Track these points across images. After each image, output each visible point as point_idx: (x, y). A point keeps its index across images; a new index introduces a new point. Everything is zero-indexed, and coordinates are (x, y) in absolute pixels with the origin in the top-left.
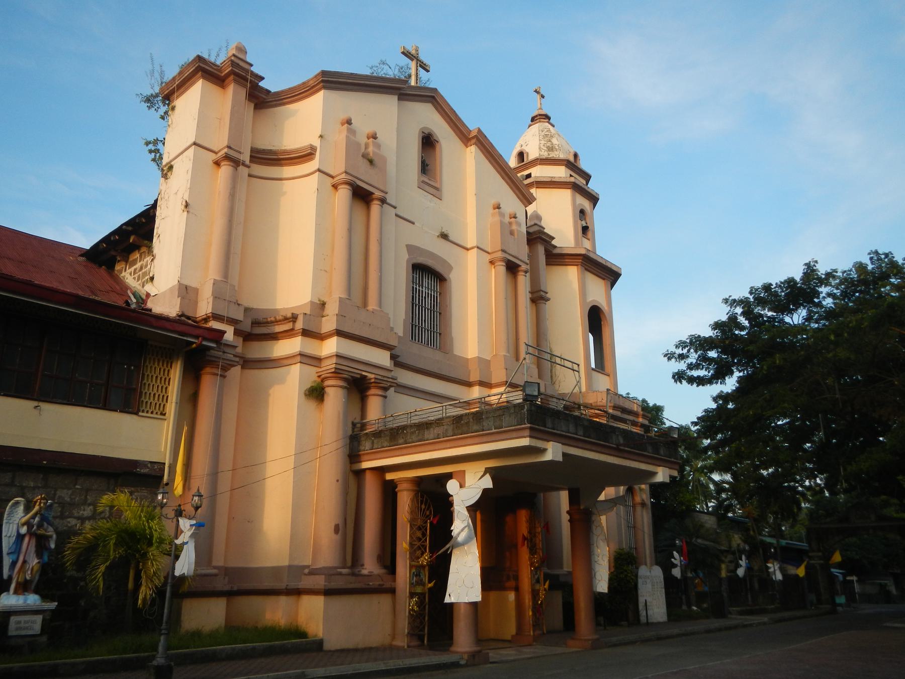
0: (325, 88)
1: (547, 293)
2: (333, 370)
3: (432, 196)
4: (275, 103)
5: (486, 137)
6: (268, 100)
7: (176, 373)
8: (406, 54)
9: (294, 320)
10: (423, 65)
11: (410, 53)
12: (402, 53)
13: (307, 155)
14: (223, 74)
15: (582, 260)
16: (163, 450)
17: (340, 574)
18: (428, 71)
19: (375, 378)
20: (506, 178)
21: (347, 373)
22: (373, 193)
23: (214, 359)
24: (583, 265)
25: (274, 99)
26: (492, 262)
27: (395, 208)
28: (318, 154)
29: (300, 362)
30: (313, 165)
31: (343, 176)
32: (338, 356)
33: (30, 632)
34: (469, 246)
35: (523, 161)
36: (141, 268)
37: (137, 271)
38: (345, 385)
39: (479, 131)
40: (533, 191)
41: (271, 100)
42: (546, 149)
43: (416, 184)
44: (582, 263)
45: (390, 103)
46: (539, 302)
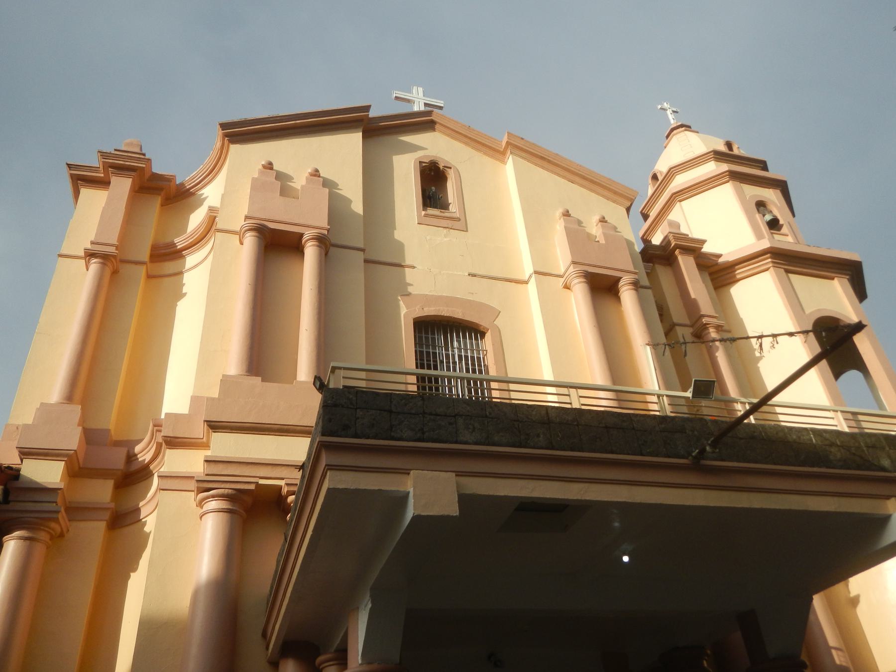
0: (233, 142)
5: (522, 139)
15: (771, 258)
19: (287, 484)
20: (577, 179)
21: (223, 486)
23: (15, 515)
24: (776, 265)
26: (567, 287)
27: (363, 250)
34: (526, 278)
35: (658, 180)
38: (230, 507)
43: (417, 222)
44: (773, 262)
46: (704, 334)
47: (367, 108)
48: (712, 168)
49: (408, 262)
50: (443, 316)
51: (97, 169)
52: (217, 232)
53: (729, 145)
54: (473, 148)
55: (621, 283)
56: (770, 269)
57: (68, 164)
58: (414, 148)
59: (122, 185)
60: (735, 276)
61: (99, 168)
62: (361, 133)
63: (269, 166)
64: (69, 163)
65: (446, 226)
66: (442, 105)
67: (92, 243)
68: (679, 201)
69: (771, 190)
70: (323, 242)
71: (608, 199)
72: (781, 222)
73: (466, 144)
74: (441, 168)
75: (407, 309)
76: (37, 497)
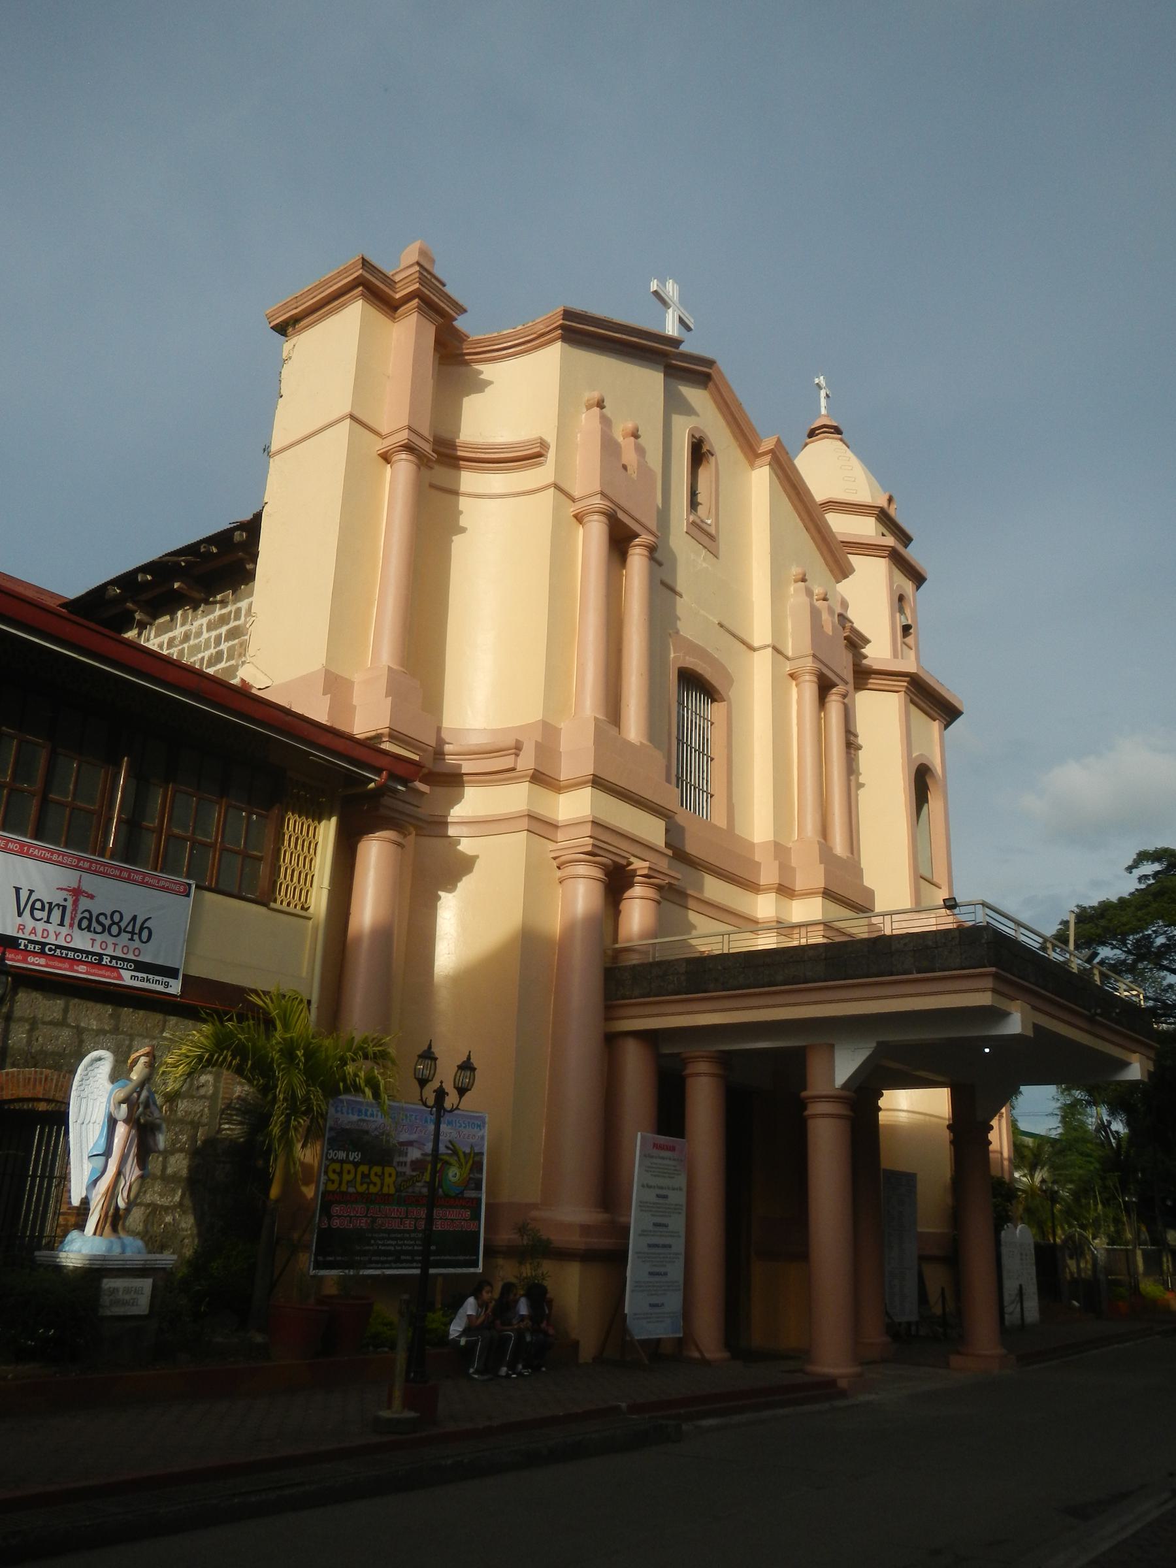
2: (589, 848)
7: (327, 832)
9: (517, 751)
13: (532, 456)
14: (397, 296)
15: (908, 683)
16: (304, 974)
24: (908, 691)
28: (551, 455)
29: (528, 830)
30: (543, 474)
31: (597, 501)
32: (595, 823)
33: (134, 1311)
34: (756, 644)
36: (187, 637)
37: (177, 642)
40: (853, 559)
44: (907, 687)
45: (651, 380)
48: (866, 528)
49: (679, 589)
50: (696, 672)
51: (392, 284)
52: (555, 487)
53: (890, 500)
54: (733, 432)
55: (834, 690)
56: (900, 693)
57: (363, 258)
58: (689, 410)
60: (867, 684)
61: (396, 283)
62: (661, 375)
64: (367, 258)
66: (692, 326)
69: (911, 582)
70: (652, 550)
71: (827, 565)
72: (912, 631)
73: (728, 423)
74: (704, 450)
75: (674, 653)
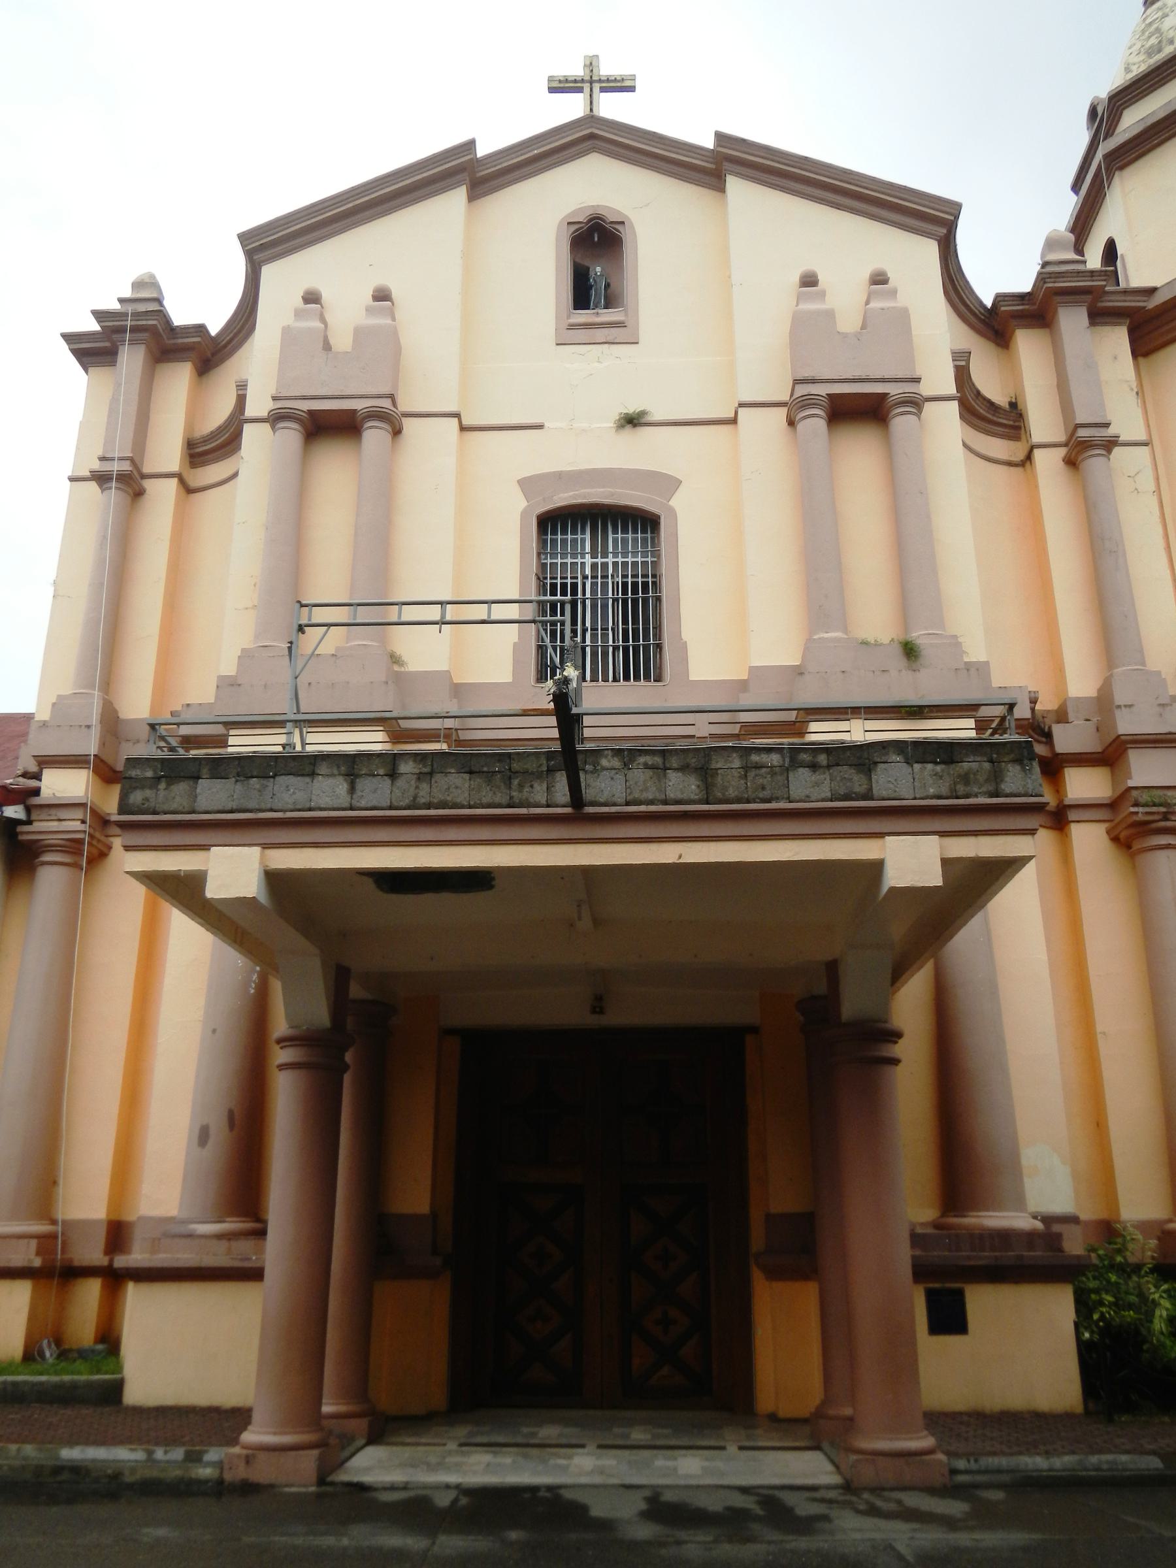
1: (1107, 425)
3: (606, 345)
4: (236, 340)
5: (744, 141)
6: (224, 342)
8: (561, 86)
10: (619, 84)
11: (567, 81)
12: (549, 92)
17: (191, 1236)
18: (631, 89)
22: (354, 411)
25: (232, 335)
27: (457, 415)
39: (720, 137)
41: (228, 338)
42: (1142, 57)
43: (555, 344)
46: (1080, 459)
47: (470, 145)
59: (131, 358)
63: (312, 298)
65: (605, 341)
67: (103, 459)
68: (1116, 169)
76: (63, 814)
